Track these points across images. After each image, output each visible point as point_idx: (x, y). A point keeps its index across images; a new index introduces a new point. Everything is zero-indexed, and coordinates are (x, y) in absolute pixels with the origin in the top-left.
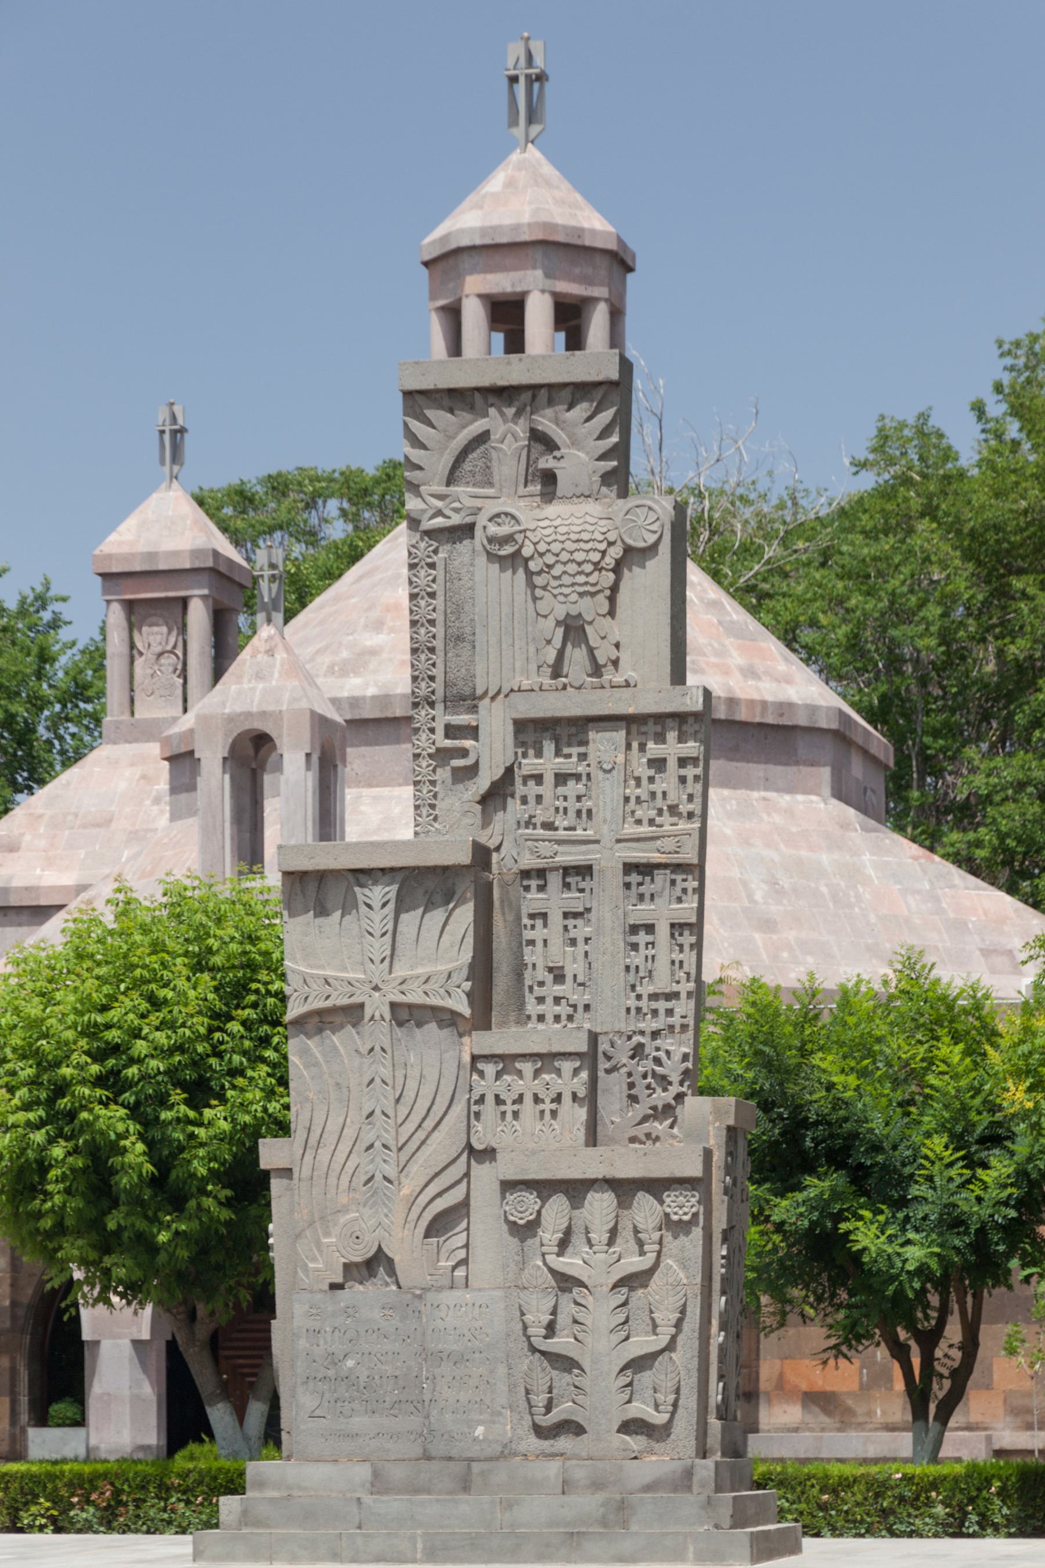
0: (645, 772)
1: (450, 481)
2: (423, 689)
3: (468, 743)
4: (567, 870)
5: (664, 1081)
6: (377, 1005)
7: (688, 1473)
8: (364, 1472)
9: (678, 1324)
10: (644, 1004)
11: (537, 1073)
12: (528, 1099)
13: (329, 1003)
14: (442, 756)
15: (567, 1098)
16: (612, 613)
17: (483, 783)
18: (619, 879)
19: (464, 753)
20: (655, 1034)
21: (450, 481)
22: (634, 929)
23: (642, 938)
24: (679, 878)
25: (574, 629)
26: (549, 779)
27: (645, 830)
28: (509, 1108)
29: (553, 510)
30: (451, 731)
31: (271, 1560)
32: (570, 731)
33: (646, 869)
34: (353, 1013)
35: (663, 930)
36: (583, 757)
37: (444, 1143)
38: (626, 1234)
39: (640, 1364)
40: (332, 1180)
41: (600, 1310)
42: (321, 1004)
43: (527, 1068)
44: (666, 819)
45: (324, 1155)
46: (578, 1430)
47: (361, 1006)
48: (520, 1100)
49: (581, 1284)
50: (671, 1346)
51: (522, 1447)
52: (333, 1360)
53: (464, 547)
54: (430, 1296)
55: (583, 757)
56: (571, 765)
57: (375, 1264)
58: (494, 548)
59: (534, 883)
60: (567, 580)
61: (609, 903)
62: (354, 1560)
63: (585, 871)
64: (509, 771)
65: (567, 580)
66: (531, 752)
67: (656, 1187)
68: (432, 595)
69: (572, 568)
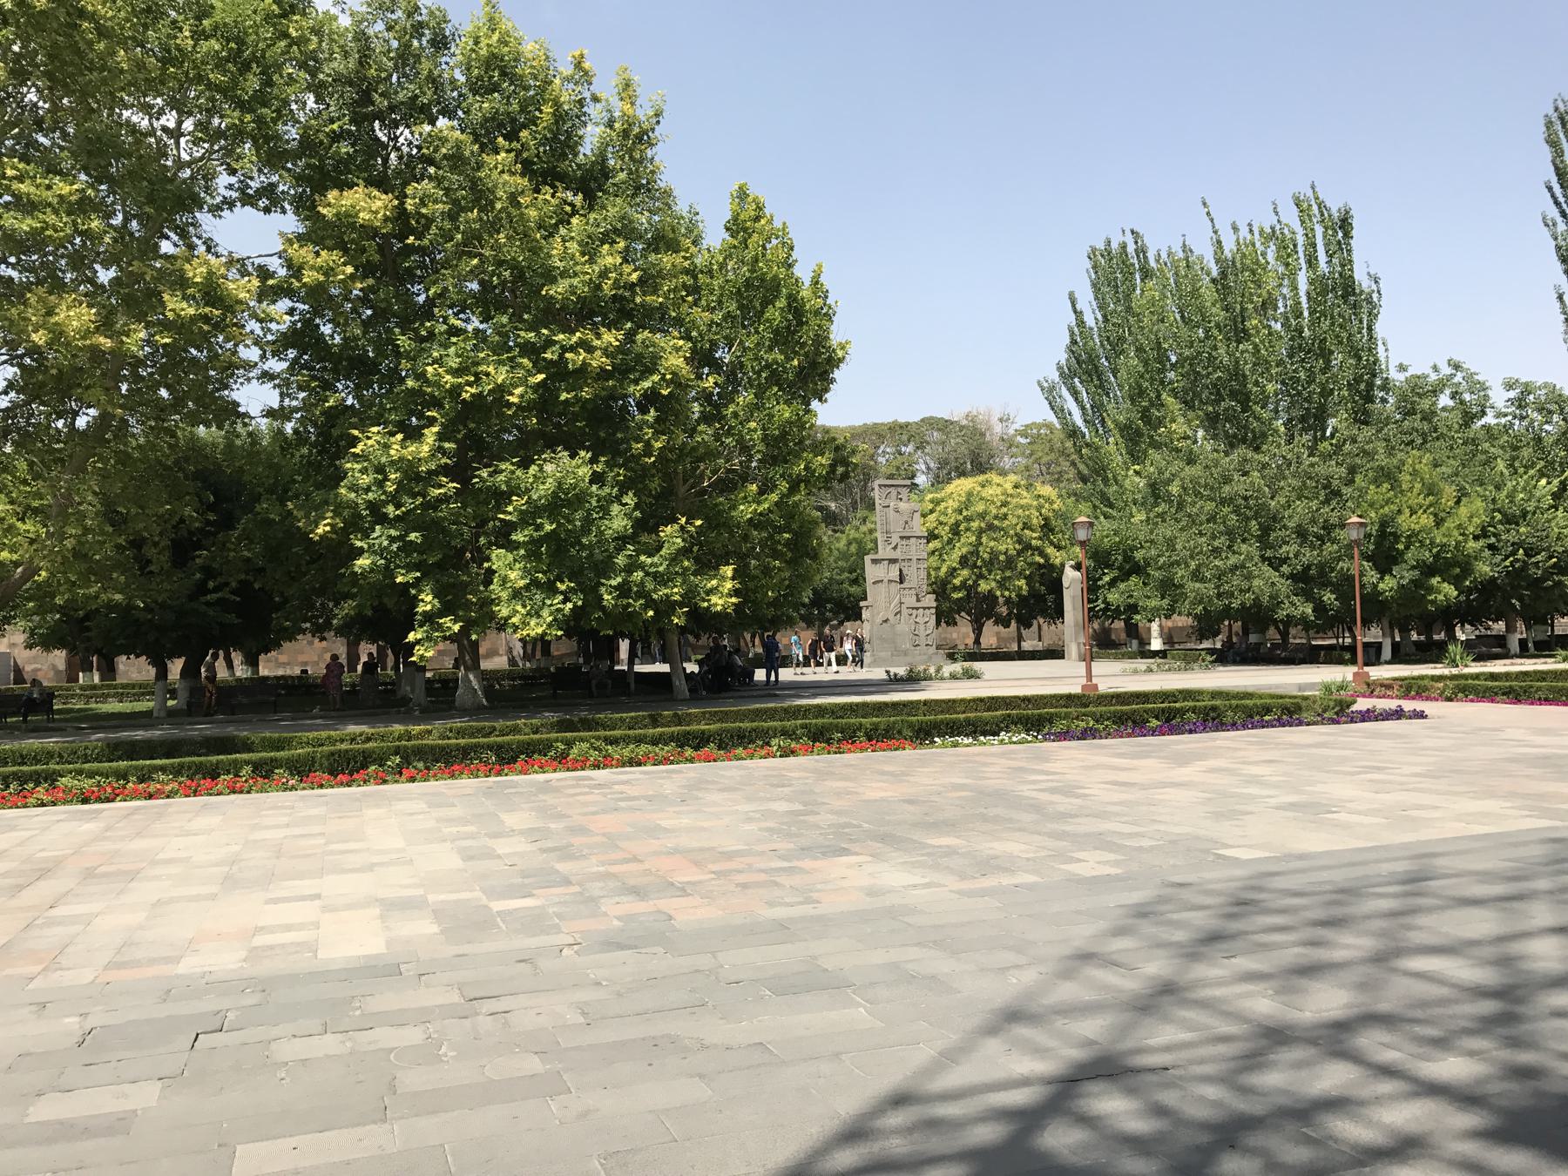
32: (908, 538)
37: (896, 601)
41: (922, 627)
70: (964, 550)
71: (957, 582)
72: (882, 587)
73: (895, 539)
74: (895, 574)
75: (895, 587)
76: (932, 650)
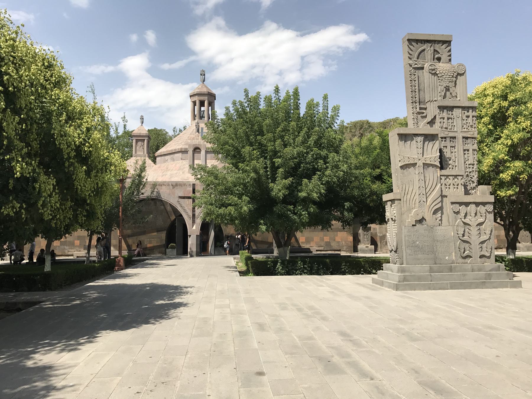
0: (464, 118)
1: (418, 59)
2: (414, 100)
3: (424, 111)
4: (451, 137)
5: (473, 182)
6: (420, 163)
7: (499, 266)
8: (427, 267)
9: (491, 234)
10: (467, 166)
11: (453, 179)
12: (452, 185)
13: (409, 163)
14: (419, 113)
15: (460, 184)
16: (455, 86)
17: (429, 119)
18: (461, 140)
19: (423, 113)
20: (470, 172)
21: (418, 59)
22: (464, 150)
23: (466, 152)
24: (473, 140)
25: (447, 89)
26: (446, 118)
27: (465, 130)
28: (448, 186)
29: (441, 64)
30: (421, 108)
31: (415, 290)
32: (451, 108)
33: (467, 138)
34: (414, 165)
35: (471, 151)
36: (452, 114)
37: (436, 193)
38: (478, 214)
39: (483, 242)
40: (411, 202)
41: (474, 231)
42: (407, 163)
43: (451, 178)
44: (470, 128)
45: (409, 196)
46: (471, 257)
47: (416, 163)
48: (450, 185)
49: (469, 225)
50: (489, 239)
51: (458, 262)
52: (414, 242)
53: (421, 71)
54: (435, 228)
55: (452, 114)
56: (450, 116)
57: (421, 221)
58: (430, 71)
59: (444, 140)
60: (446, 79)
61: (459, 144)
62: (434, 289)
63: (455, 138)
64: (435, 117)
65: (446, 79)
66: (441, 112)
67: (484, 204)
68: (415, 81)
69: (448, 76)
70: (516, 137)
71: (505, 176)
72: (414, 174)
73: (432, 110)
74: (432, 153)
75: (433, 174)
76: (490, 264)
